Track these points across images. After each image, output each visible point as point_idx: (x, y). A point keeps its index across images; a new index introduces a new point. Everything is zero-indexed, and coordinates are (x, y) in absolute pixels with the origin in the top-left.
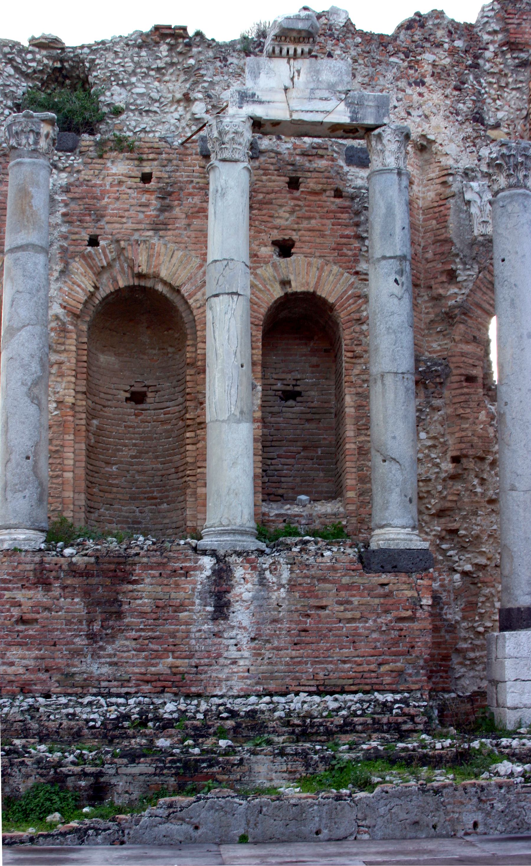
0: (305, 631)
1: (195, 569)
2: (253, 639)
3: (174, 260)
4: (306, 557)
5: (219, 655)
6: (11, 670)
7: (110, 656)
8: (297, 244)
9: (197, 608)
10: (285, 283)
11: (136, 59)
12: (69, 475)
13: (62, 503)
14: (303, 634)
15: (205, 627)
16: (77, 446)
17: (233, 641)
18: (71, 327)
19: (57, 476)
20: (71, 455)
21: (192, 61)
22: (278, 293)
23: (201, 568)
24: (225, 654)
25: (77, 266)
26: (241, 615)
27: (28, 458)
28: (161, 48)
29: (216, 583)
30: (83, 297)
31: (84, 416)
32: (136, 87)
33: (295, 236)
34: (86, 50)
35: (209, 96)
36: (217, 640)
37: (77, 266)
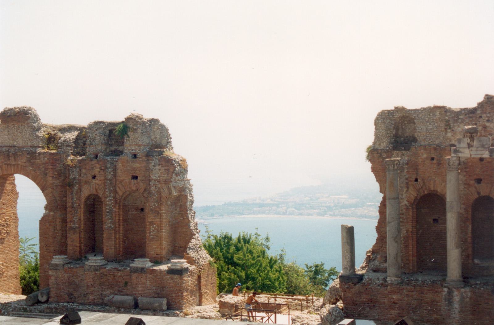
0: (475, 311)
1: (442, 291)
2: (459, 312)
3: (442, 186)
4: (475, 289)
5: (450, 316)
6: (391, 316)
7: (419, 314)
8: (483, 180)
9: (443, 302)
10: (479, 193)
11: (429, 117)
12: (411, 253)
13: (409, 261)
14: (474, 311)
15: (446, 308)
16: (413, 243)
17: (453, 312)
18: (410, 207)
19: (407, 253)
20: (411, 247)
21: (447, 118)
22: (476, 196)
23: (444, 291)
24: (451, 316)
25: (411, 188)
26: (456, 306)
27: (395, 258)
28: (437, 113)
29: (449, 296)
30: (413, 198)
31: (415, 234)
32: (429, 126)
33: (482, 177)
34: (413, 112)
35: (453, 130)
36: (449, 311)
37: (411, 188)
